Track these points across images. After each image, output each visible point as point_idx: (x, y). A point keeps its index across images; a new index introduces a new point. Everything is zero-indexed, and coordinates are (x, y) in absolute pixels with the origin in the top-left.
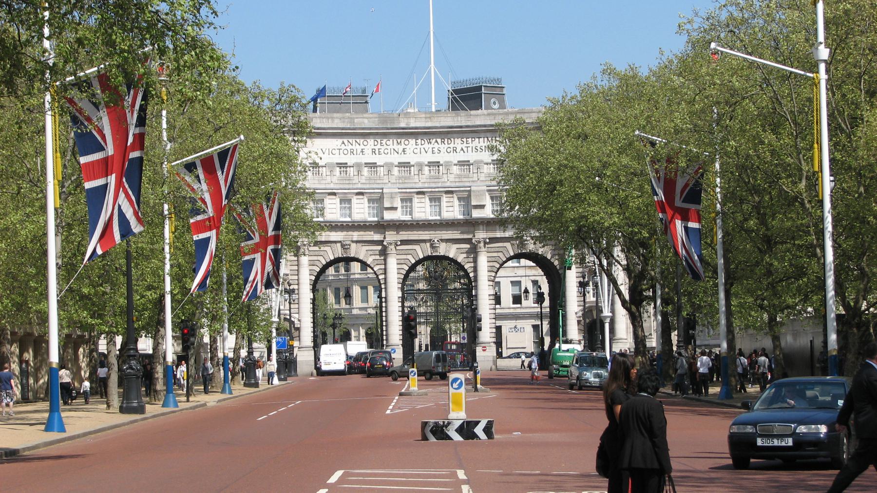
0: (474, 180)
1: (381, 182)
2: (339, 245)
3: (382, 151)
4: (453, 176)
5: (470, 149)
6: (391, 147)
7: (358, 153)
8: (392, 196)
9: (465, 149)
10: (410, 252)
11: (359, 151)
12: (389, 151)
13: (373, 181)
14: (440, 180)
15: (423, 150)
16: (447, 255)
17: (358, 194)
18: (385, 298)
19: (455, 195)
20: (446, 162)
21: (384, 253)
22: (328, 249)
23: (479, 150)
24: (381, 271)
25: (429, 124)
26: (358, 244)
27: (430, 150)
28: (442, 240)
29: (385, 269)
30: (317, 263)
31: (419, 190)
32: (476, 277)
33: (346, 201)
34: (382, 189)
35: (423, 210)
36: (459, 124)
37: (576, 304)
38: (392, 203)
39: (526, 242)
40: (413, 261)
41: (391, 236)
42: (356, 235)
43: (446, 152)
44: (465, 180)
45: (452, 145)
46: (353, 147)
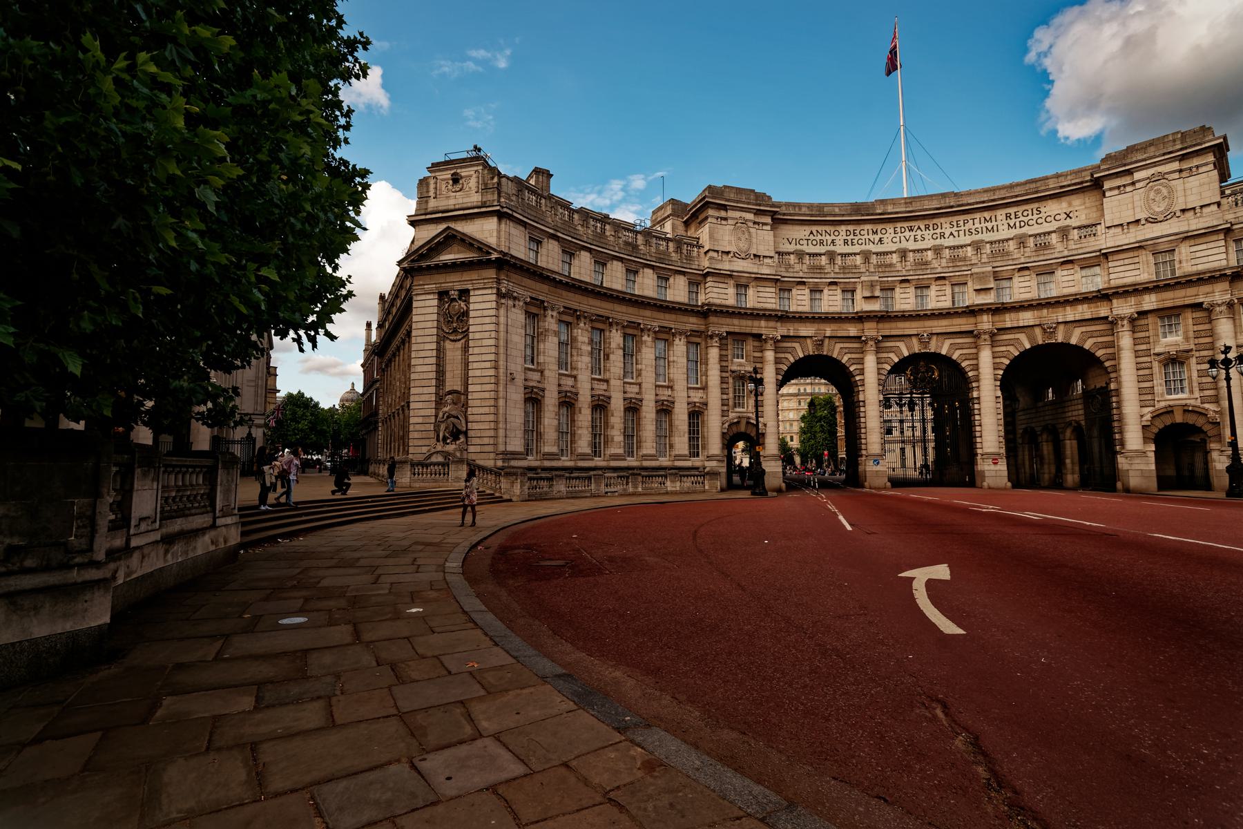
0: (973, 262)
1: (858, 271)
2: (809, 341)
3: (855, 241)
4: (944, 260)
5: (962, 233)
6: (866, 236)
7: (829, 243)
8: (872, 285)
9: (956, 234)
10: (894, 349)
11: (829, 243)
12: (864, 241)
14: (929, 267)
15: (903, 238)
16: (938, 351)
17: (831, 284)
18: (864, 401)
19: (947, 282)
20: (934, 246)
22: (797, 345)
23: (974, 232)
24: (858, 372)
27: (912, 238)
28: (932, 334)
30: (784, 360)
31: (903, 278)
33: (816, 290)
35: (908, 301)
36: (947, 205)
38: (872, 292)
40: (896, 360)
41: (870, 330)
42: (829, 330)
43: (931, 240)
44: (960, 263)
45: (939, 231)
46: (823, 238)
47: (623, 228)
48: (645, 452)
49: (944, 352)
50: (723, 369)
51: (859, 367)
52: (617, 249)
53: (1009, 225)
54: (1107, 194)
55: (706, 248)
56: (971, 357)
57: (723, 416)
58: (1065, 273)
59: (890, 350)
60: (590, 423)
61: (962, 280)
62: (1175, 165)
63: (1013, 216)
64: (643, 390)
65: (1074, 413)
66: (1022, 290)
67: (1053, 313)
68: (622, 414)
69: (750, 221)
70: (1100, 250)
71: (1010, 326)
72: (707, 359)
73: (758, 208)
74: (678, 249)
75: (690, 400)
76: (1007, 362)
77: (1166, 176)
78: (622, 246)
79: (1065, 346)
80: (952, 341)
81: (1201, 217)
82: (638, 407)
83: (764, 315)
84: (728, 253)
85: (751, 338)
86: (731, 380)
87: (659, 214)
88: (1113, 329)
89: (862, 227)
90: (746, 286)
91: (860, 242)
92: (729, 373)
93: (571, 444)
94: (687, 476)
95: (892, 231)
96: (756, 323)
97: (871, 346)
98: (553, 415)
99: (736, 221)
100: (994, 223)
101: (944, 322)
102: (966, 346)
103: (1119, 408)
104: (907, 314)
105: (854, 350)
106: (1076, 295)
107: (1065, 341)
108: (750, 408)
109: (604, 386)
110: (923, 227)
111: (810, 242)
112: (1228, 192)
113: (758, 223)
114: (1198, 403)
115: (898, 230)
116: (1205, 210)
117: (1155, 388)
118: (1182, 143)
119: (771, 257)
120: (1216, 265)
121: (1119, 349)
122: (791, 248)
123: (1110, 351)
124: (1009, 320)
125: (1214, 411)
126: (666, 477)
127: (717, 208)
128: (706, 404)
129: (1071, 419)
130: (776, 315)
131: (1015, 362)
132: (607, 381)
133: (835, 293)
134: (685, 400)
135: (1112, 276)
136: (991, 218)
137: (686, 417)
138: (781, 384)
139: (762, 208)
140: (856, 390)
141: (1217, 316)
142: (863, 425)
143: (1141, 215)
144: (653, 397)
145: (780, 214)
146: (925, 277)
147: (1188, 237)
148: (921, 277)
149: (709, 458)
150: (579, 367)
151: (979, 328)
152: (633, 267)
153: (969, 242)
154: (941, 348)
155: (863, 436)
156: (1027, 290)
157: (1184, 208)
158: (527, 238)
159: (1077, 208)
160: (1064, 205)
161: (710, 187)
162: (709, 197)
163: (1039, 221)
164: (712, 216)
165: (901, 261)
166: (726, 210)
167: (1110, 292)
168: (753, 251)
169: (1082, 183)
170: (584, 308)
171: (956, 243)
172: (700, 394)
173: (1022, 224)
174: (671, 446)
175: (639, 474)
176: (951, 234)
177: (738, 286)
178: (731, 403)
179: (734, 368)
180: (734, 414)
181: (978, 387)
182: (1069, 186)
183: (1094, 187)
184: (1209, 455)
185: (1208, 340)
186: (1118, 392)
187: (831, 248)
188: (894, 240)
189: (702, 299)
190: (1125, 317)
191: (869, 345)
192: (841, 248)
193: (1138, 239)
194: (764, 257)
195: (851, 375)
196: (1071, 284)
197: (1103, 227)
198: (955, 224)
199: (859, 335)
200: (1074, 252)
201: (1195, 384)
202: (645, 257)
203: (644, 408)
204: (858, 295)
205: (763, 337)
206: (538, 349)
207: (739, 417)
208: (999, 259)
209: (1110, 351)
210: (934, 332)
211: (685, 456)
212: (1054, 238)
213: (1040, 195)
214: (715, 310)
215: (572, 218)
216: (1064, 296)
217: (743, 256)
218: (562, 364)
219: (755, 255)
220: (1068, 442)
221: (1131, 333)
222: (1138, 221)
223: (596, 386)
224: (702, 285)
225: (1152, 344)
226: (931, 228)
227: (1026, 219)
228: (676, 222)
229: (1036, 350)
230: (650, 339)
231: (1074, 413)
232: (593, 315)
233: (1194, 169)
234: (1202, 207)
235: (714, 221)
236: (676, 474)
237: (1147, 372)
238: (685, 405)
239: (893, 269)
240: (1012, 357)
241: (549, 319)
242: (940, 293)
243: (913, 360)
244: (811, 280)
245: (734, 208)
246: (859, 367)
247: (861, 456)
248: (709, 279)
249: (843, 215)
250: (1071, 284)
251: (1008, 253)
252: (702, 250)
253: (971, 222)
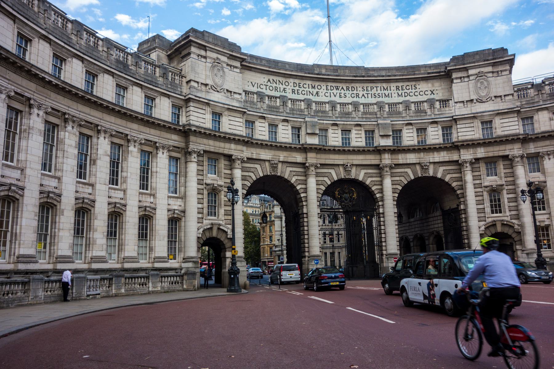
1: (303, 113)
2: (267, 164)
3: (300, 92)
5: (370, 95)
6: (307, 89)
7: (281, 90)
8: (314, 125)
9: (366, 95)
11: (282, 90)
12: (306, 92)
13: (295, 112)
15: (332, 94)
16: (357, 178)
17: (284, 121)
21: (306, 175)
22: (258, 166)
24: (302, 191)
25: (337, 74)
26: (284, 165)
27: (338, 94)
28: (353, 165)
29: (306, 188)
30: (248, 178)
31: (334, 122)
32: (382, 197)
35: (337, 139)
37: (477, 219)
39: (427, 167)
40: (329, 183)
41: (312, 158)
42: (282, 156)
43: (350, 97)
45: (355, 92)
46: (277, 85)
47: (115, 47)
48: (127, 254)
49: (361, 178)
50: (200, 182)
51: (303, 186)
52: (108, 64)
53: (398, 94)
54: (455, 81)
55: (188, 79)
56: (378, 183)
57: (198, 223)
58: (433, 129)
60: (73, 225)
61: (371, 128)
62: (490, 69)
63: (400, 88)
64: (128, 196)
65: (436, 226)
66: (409, 139)
67: (427, 155)
68: (106, 218)
69: (224, 62)
70: (452, 117)
71: (401, 162)
72: (186, 172)
73: (231, 53)
74: (164, 75)
75: (170, 207)
76: (400, 188)
77: (486, 74)
78: (113, 63)
79: (434, 179)
80: (366, 171)
81: (505, 102)
82: (122, 212)
83: (234, 139)
84: (206, 85)
85: (222, 158)
86: (205, 192)
87: (145, 46)
88: (460, 169)
89: (305, 82)
90: (220, 115)
91: (303, 92)
92: (204, 186)
93: (50, 246)
94: (168, 277)
95: (325, 87)
96: (227, 145)
98: (32, 215)
99: (213, 61)
100: (389, 91)
101: (361, 157)
102: (374, 175)
103: (466, 222)
104: (337, 149)
105: (300, 174)
106: (440, 144)
107: (434, 175)
108: (220, 216)
109: (90, 190)
110: (345, 88)
111: (268, 87)
112: (516, 89)
113: (231, 66)
114: (508, 219)
115: (329, 87)
116: (507, 98)
117: (486, 209)
118: (493, 56)
119: (240, 94)
120: (514, 132)
121: (465, 182)
122: (255, 89)
123: (459, 183)
124: (402, 158)
125: (518, 225)
126: (148, 278)
127: (198, 48)
128: (184, 212)
129: (433, 230)
130: (244, 140)
131: (405, 187)
132: (92, 185)
133: (287, 128)
134: (166, 207)
135: (460, 134)
136: (387, 88)
137: (166, 223)
138: (246, 196)
139: (234, 54)
140: (301, 204)
141: (516, 164)
142: (306, 232)
143: (474, 97)
144: (136, 204)
145: (246, 62)
146: (348, 123)
147: (500, 114)
148: (345, 123)
149: (186, 260)
150: (65, 169)
151: (383, 162)
152: (123, 83)
153: (375, 102)
154: (359, 175)
155: (306, 241)
156: (411, 138)
157: (496, 95)
158: (16, 34)
159: (437, 88)
160: (430, 85)
161: (192, 28)
162: (192, 37)
163: (416, 94)
164: (194, 53)
165: (332, 110)
166: (206, 51)
167: (460, 144)
168: (226, 87)
169: (440, 72)
170: (73, 112)
171: (367, 102)
172: (179, 202)
173: (406, 94)
174: (151, 249)
175: (123, 276)
176: (363, 95)
177: (214, 114)
178: (205, 211)
179: (209, 182)
180: (207, 221)
181: (383, 205)
182: (433, 73)
183: (446, 76)
184: (515, 253)
186: (465, 211)
187: (283, 94)
188: (326, 94)
189: (183, 120)
190: (468, 161)
191: (311, 170)
192: (290, 95)
193: (474, 111)
194: (234, 93)
195: (297, 193)
196: (437, 137)
197: (453, 102)
198: (365, 88)
199: (304, 162)
200: (438, 117)
201: (507, 207)
202: (134, 76)
203: (128, 213)
204: (303, 132)
205: (233, 157)
206: (19, 146)
207: (212, 224)
208: (394, 116)
209: (459, 183)
210: (354, 163)
211: (163, 258)
212: (426, 106)
213: (416, 76)
214: (195, 131)
215: (64, 26)
216: (433, 145)
217: (218, 89)
218: (46, 165)
219: (227, 90)
220: (431, 246)
221: (471, 172)
222: (472, 101)
223: (80, 190)
224: (184, 109)
225: (482, 180)
226: (350, 89)
227: (408, 91)
228: (160, 54)
229: (417, 180)
230: (135, 150)
231: (436, 226)
232: (81, 120)
233: (500, 73)
234: (505, 96)
235: (196, 57)
236: (158, 275)
237: (480, 198)
238: (166, 212)
239: (326, 115)
240: (403, 185)
241: (34, 117)
242: (358, 136)
243: (340, 182)
244: (269, 116)
245: (212, 50)
246: (303, 186)
247: (305, 257)
248: (191, 104)
249: (292, 71)
250: (437, 137)
251: (399, 113)
252: (184, 80)
253: (375, 88)
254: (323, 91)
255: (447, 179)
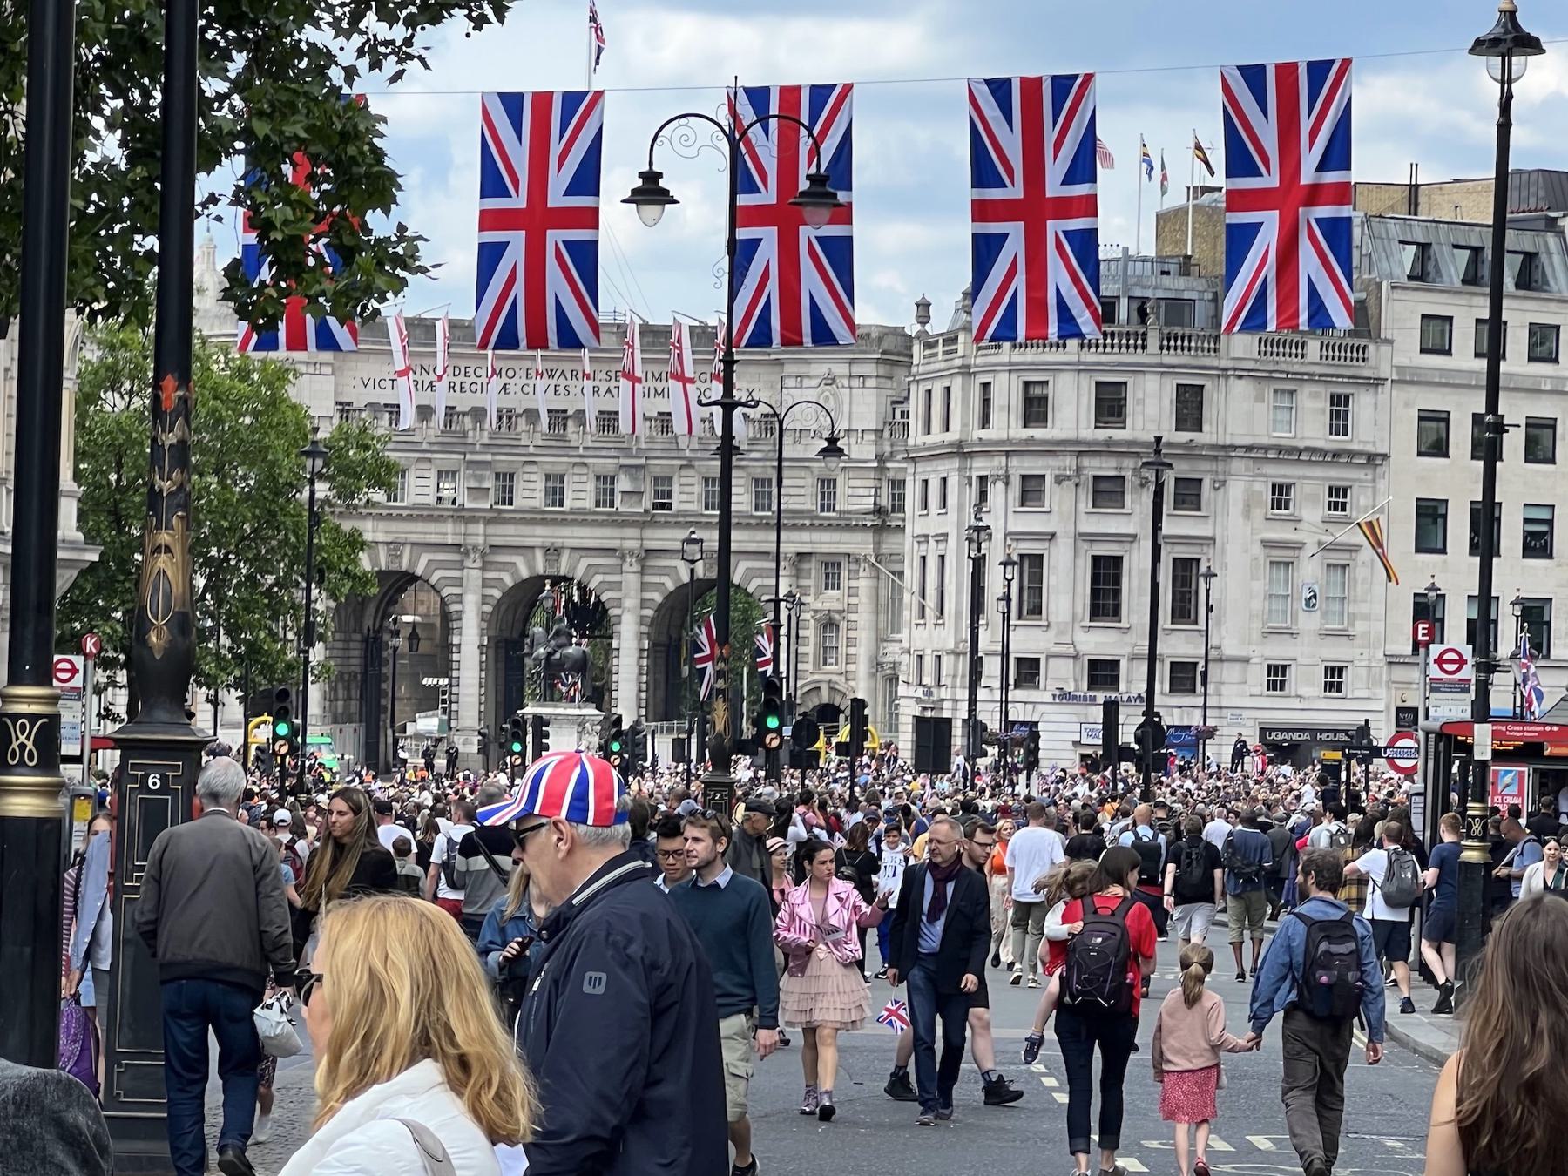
3: (466, 386)
9: (614, 391)
12: (479, 387)
26: (415, 547)
27: (552, 388)
34: (465, 454)
51: (457, 591)
59: (504, 567)
69: (299, 362)
95: (523, 373)
97: (473, 562)
154: (575, 568)
176: (609, 390)
185: (853, 600)
199: (462, 542)
242: (581, 487)
246: (457, 591)
254: (520, 380)
255: (750, 590)
